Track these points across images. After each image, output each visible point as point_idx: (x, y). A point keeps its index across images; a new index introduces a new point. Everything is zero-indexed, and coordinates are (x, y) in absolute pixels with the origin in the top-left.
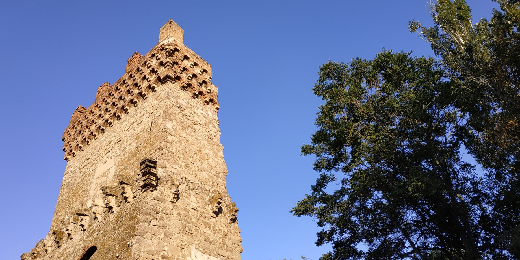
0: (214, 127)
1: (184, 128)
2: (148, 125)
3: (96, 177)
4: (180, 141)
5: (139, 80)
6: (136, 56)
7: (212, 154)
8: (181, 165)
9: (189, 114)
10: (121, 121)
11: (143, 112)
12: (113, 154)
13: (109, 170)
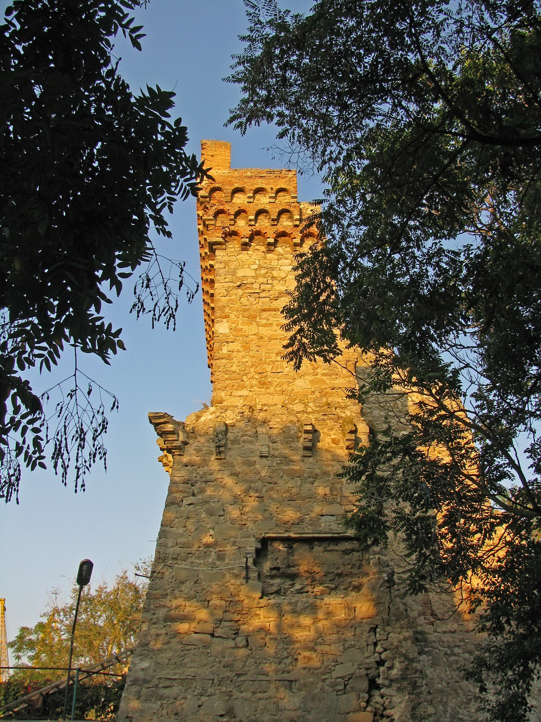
1: (252, 318)
8: (252, 386)
9: (262, 287)
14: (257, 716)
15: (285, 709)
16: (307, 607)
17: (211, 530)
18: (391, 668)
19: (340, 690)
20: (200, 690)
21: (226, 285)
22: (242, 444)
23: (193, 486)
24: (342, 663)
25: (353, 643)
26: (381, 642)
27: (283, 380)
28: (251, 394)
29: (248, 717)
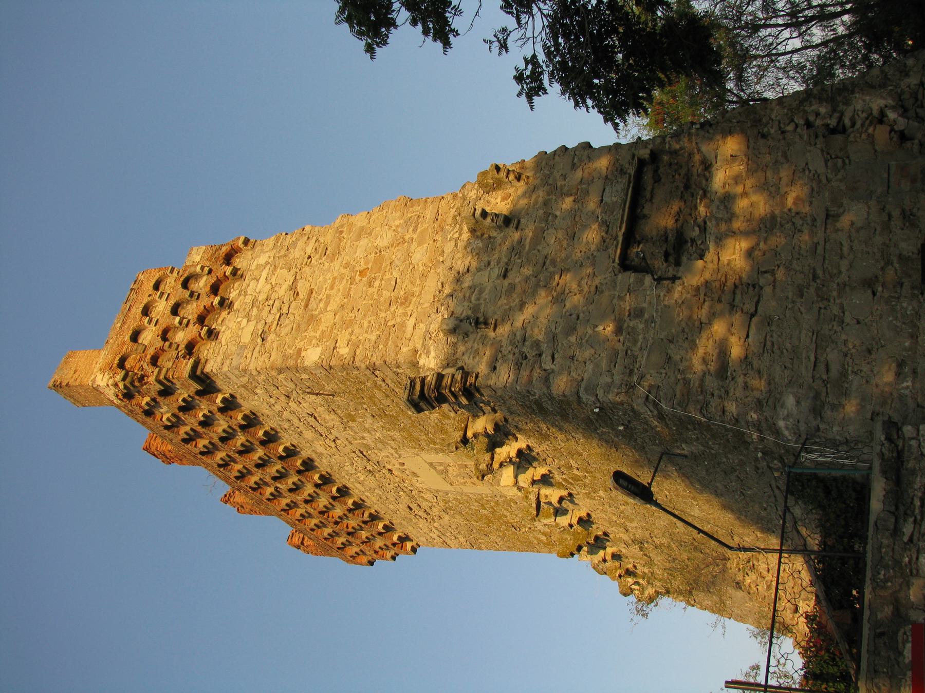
0: (294, 244)
1: (312, 319)
2: (319, 400)
3: (449, 488)
4: (347, 324)
5: (212, 435)
6: (153, 449)
7: (364, 242)
8: (405, 314)
9: (274, 310)
10: (314, 456)
11: (286, 414)
12: (394, 461)
13: (431, 464)
14: (876, 250)
15: (867, 219)
16: (725, 206)
17: (597, 329)
18: (817, 114)
19: (844, 162)
20: (835, 323)
21: (256, 354)
22: (482, 301)
23: (526, 357)
24: (807, 164)
25: (780, 154)
26: (782, 126)
27: (408, 276)
28: (415, 315)
29: (877, 261)
